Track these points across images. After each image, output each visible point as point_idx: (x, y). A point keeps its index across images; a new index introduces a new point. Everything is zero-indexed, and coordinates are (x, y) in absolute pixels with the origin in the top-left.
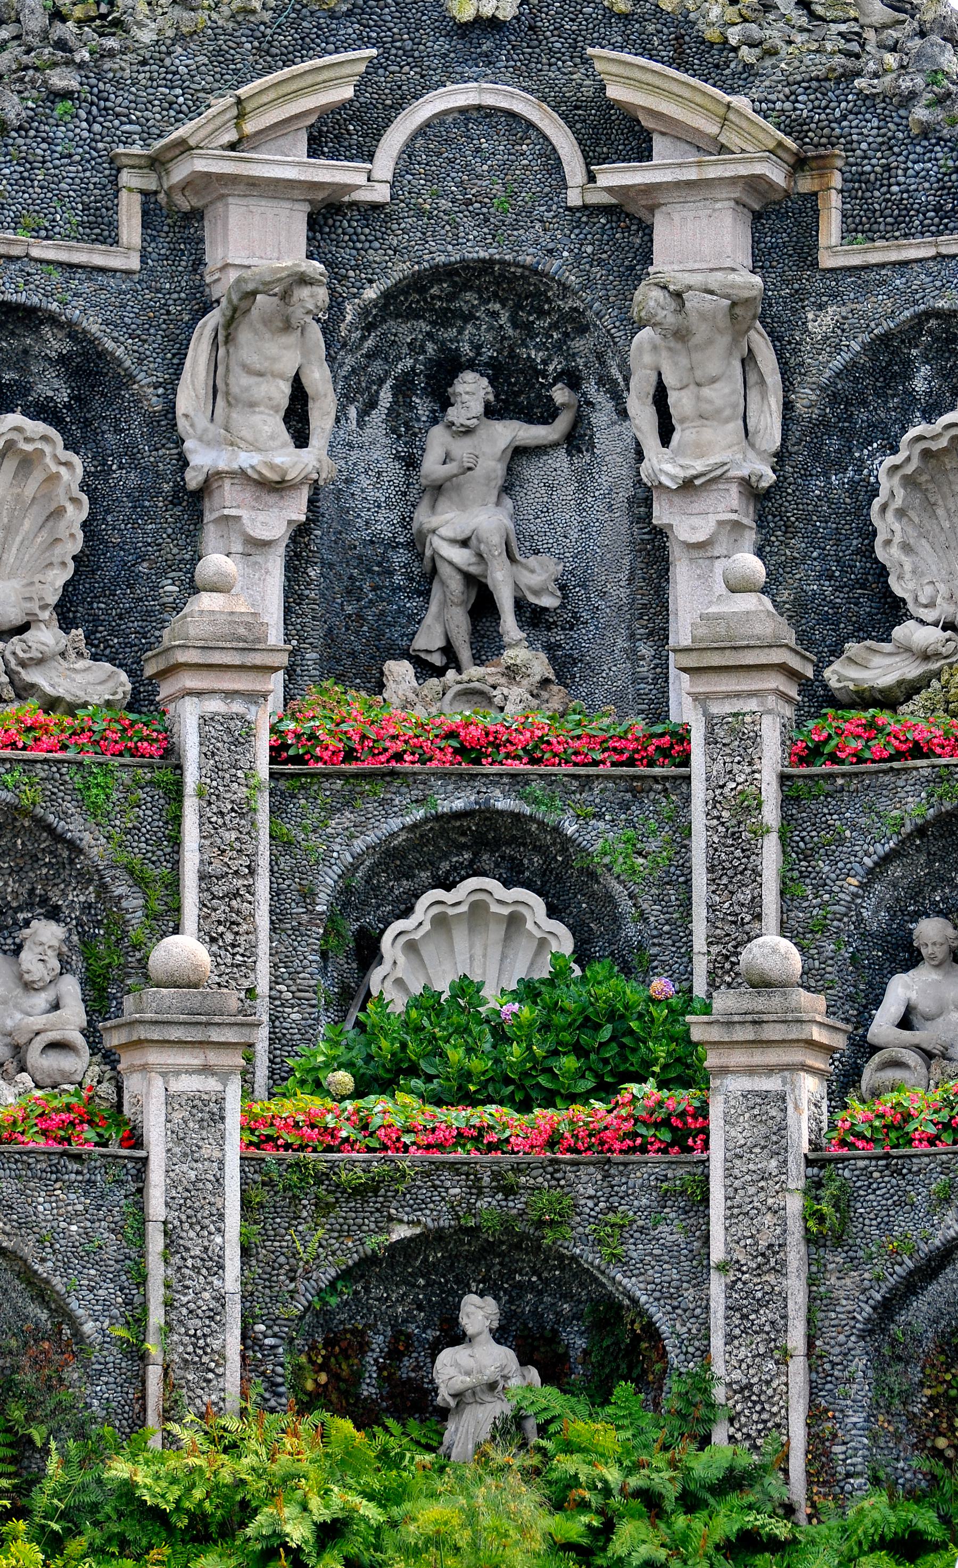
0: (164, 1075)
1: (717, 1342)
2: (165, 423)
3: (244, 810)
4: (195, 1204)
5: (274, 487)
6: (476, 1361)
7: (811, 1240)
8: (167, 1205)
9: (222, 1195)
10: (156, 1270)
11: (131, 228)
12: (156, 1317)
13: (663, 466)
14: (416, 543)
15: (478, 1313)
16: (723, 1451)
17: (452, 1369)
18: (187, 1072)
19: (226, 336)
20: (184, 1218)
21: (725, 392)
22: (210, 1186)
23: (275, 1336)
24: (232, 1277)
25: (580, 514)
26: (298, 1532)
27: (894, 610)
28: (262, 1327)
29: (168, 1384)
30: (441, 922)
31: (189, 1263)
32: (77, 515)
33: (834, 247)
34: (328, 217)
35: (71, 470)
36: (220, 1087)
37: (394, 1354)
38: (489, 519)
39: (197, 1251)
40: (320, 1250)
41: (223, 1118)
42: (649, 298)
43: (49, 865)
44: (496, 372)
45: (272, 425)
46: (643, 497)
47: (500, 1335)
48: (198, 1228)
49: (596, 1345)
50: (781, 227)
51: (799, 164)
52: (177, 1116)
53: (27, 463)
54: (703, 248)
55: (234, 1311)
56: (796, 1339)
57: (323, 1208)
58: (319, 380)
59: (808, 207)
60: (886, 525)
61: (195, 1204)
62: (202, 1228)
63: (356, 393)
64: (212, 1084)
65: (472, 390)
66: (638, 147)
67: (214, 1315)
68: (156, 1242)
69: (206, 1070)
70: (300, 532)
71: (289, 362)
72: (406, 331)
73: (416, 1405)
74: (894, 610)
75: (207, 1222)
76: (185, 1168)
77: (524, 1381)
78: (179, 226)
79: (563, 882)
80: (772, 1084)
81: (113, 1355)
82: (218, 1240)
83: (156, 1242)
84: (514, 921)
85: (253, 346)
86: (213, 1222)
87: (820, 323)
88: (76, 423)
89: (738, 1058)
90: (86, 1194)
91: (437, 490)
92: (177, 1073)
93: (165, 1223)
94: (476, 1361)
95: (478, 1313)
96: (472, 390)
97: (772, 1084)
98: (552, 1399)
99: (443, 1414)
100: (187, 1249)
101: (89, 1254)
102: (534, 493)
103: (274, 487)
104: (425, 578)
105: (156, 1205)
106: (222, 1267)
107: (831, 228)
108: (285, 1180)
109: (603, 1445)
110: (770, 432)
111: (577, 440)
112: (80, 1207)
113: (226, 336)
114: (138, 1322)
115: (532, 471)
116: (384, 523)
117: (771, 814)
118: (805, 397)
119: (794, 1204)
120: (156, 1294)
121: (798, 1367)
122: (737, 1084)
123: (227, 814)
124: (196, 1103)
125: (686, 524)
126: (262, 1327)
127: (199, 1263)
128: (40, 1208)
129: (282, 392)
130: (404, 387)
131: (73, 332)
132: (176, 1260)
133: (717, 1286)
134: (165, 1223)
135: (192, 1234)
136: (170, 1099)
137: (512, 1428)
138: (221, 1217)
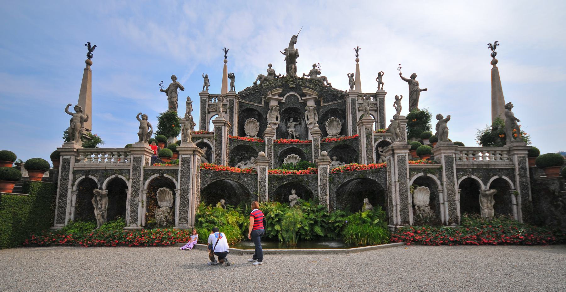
1: (319, 194)
2: (266, 120)
3: (271, 147)
4: (263, 179)
5: (275, 124)
6: (293, 196)
7: (329, 183)
10: (259, 186)
11: (263, 103)
12: (259, 191)
13: (308, 122)
14: (287, 132)
15: (293, 191)
16: (320, 205)
17: (291, 197)
19: (271, 112)
21: (313, 116)
24: (267, 187)
25: (301, 129)
26: (273, 215)
27: (328, 135)
29: (260, 199)
30: (289, 158)
32: (258, 127)
33: (322, 104)
34: (280, 102)
35: (258, 124)
37: (285, 196)
38: (293, 129)
40: (276, 184)
42: (307, 107)
44: (293, 118)
45: (275, 119)
46: (306, 125)
47: (296, 194)
49: (306, 194)
50: (317, 102)
51: (319, 97)
53: (254, 123)
54: (311, 104)
55: (267, 191)
56: (328, 193)
57: (277, 180)
58: (279, 115)
59: (320, 101)
60: (327, 127)
61: (263, 179)
63: (282, 120)
65: (292, 119)
66: (306, 96)
67: (265, 191)
68: (259, 184)
70: (277, 128)
71: (276, 114)
72: (286, 115)
73: (288, 201)
74: (328, 135)
77: (298, 198)
78: (267, 103)
79: (301, 154)
80: (325, 166)
81: (254, 196)
83: (259, 184)
84: (296, 158)
85: (273, 112)
87: (321, 111)
88: (259, 120)
89: (321, 163)
91: (289, 127)
94: (293, 196)
95: (293, 191)
96: (292, 119)
97: (325, 166)
98: (301, 200)
99: (290, 202)
101: (251, 184)
102: (297, 128)
103: (275, 124)
104: (288, 134)
105: (259, 180)
107: (322, 103)
108: (272, 178)
109: (308, 206)
110: (317, 119)
111: (300, 124)
113: (271, 112)
114: (257, 192)
115: (296, 127)
116: (285, 131)
117: (320, 147)
118: (320, 116)
119: (328, 179)
120: (259, 189)
121: (328, 196)
122: (321, 166)
123: (270, 147)
124: (263, 169)
125: (310, 127)
129: (276, 117)
130: (286, 120)
131: (258, 111)
133: (319, 188)
137: (297, 203)
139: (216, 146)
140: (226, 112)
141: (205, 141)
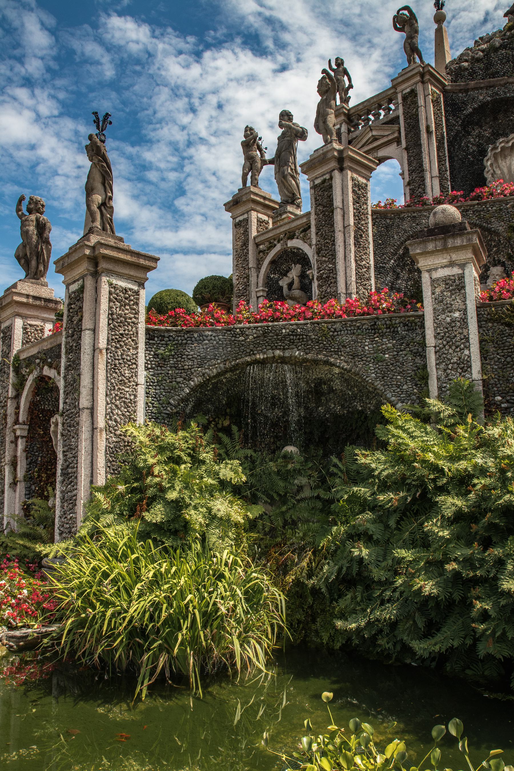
0: (429, 271)
8: (435, 337)
9: (467, 327)
18: (442, 267)
20: (445, 343)
22: (458, 324)
23: (508, 401)
28: (499, 398)
31: (450, 367)
36: (460, 272)
39: (455, 360)
41: (464, 287)
43: (495, 246)
48: (454, 347)
52: (438, 291)
62: (457, 347)
64: (456, 271)
69: (451, 264)
75: (458, 343)
76: (443, 316)
82: (466, 352)
86: (463, 343)
90: (393, 338)
92: (436, 269)
93: (435, 347)
100: (449, 359)
105: (430, 340)
106: (470, 367)
112: (389, 345)
124: (446, 280)
126: (499, 398)
127: (455, 366)
128: (367, 348)
132: (442, 366)
134: (435, 347)
135: (451, 351)
136: (433, 281)
138: (467, 339)
139: (318, 252)
140: (398, 141)
141: (292, 243)
